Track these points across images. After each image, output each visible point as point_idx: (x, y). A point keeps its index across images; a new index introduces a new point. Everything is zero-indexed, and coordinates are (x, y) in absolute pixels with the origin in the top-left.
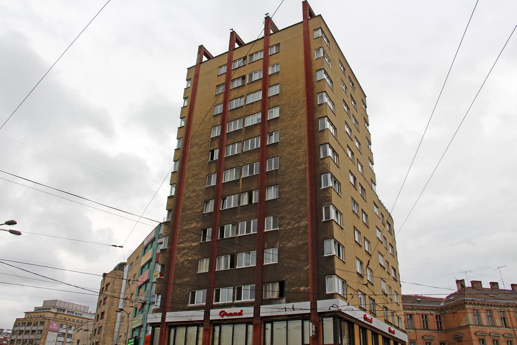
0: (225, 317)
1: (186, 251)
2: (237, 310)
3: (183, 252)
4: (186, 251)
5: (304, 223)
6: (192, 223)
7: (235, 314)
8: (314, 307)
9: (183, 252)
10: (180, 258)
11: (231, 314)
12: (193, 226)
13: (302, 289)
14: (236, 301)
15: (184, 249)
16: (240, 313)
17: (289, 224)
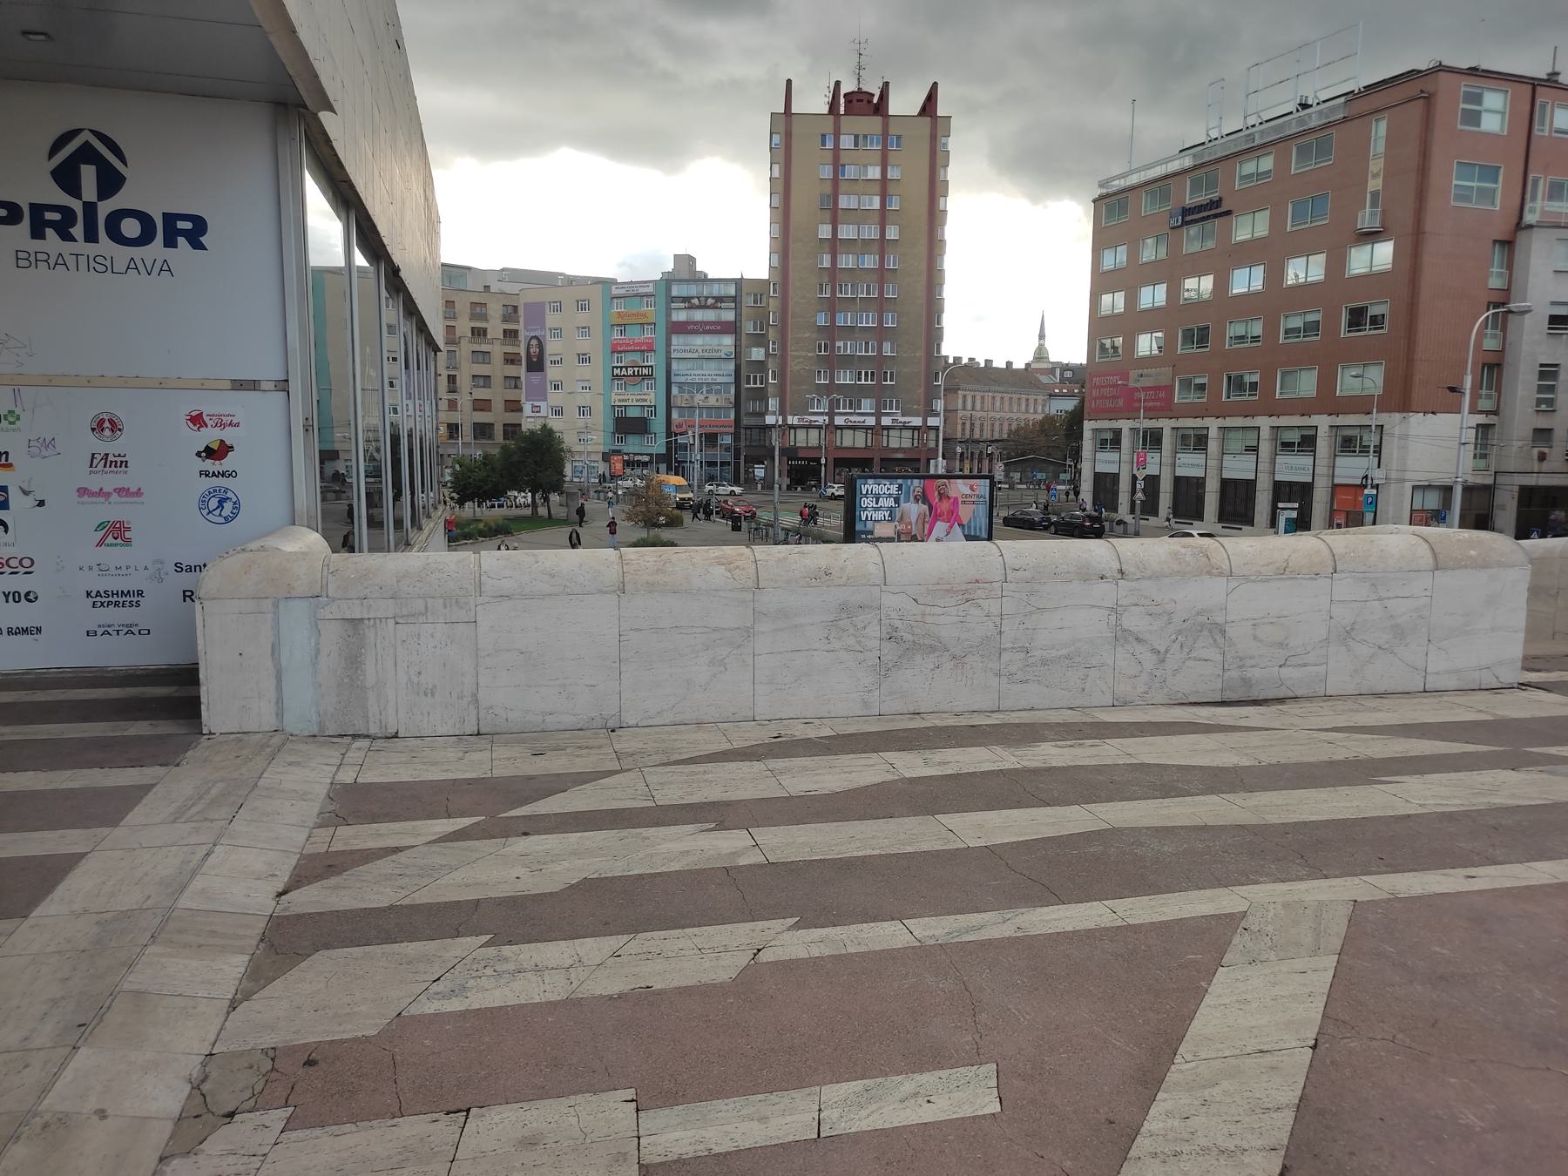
0: (849, 424)
1: (801, 360)
2: (861, 419)
3: (798, 360)
4: (801, 360)
5: (918, 354)
6: (805, 333)
7: (859, 422)
8: (925, 421)
9: (798, 360)
10: (793, 366)
11: (855, 422)
12: (806, 335)
13: (915, 407)
14: (857, 411)
15: (798, 357)
16: (864, 422)
17: (905, 352)
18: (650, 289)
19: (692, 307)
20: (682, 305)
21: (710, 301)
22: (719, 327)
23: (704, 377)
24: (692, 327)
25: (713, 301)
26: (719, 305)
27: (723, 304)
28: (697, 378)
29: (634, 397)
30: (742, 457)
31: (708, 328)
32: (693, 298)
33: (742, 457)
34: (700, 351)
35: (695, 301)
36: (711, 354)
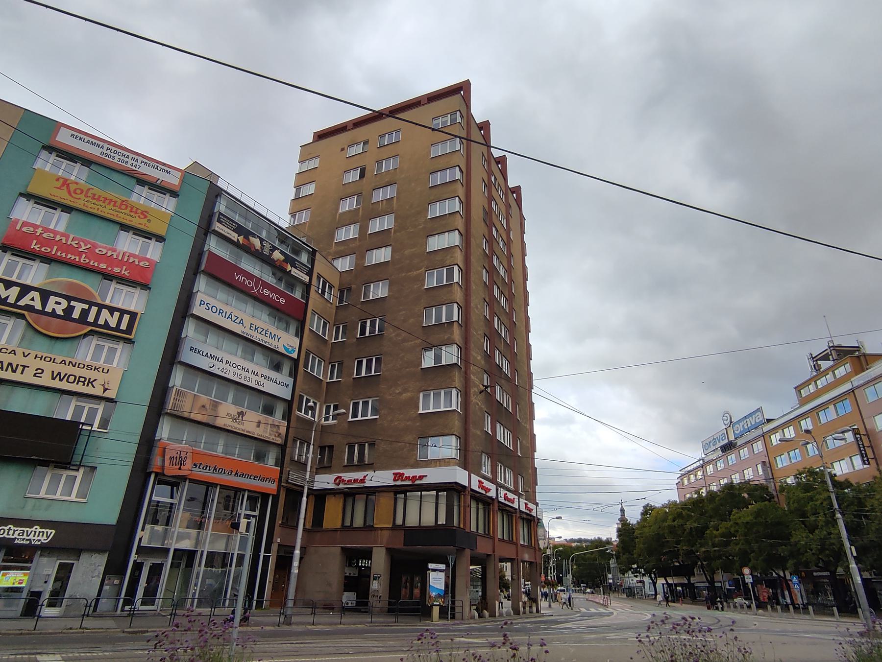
18: (173, 180)
19: (247, 249)
20: (234, 236)
21: (277, 255)
22: (282, 301)
23: (244, 374)
24: (241, 278)
25: (282, 257)
26: (289, 268)
27: (294, 270)
28: (232, 369)
29: (48, 367)
30: (274, 547)
31: (266, 292)
32: (254, 235)
33: (274, 547)
34: (247, 324)
35: (256, 242)
36: (263, 337)
